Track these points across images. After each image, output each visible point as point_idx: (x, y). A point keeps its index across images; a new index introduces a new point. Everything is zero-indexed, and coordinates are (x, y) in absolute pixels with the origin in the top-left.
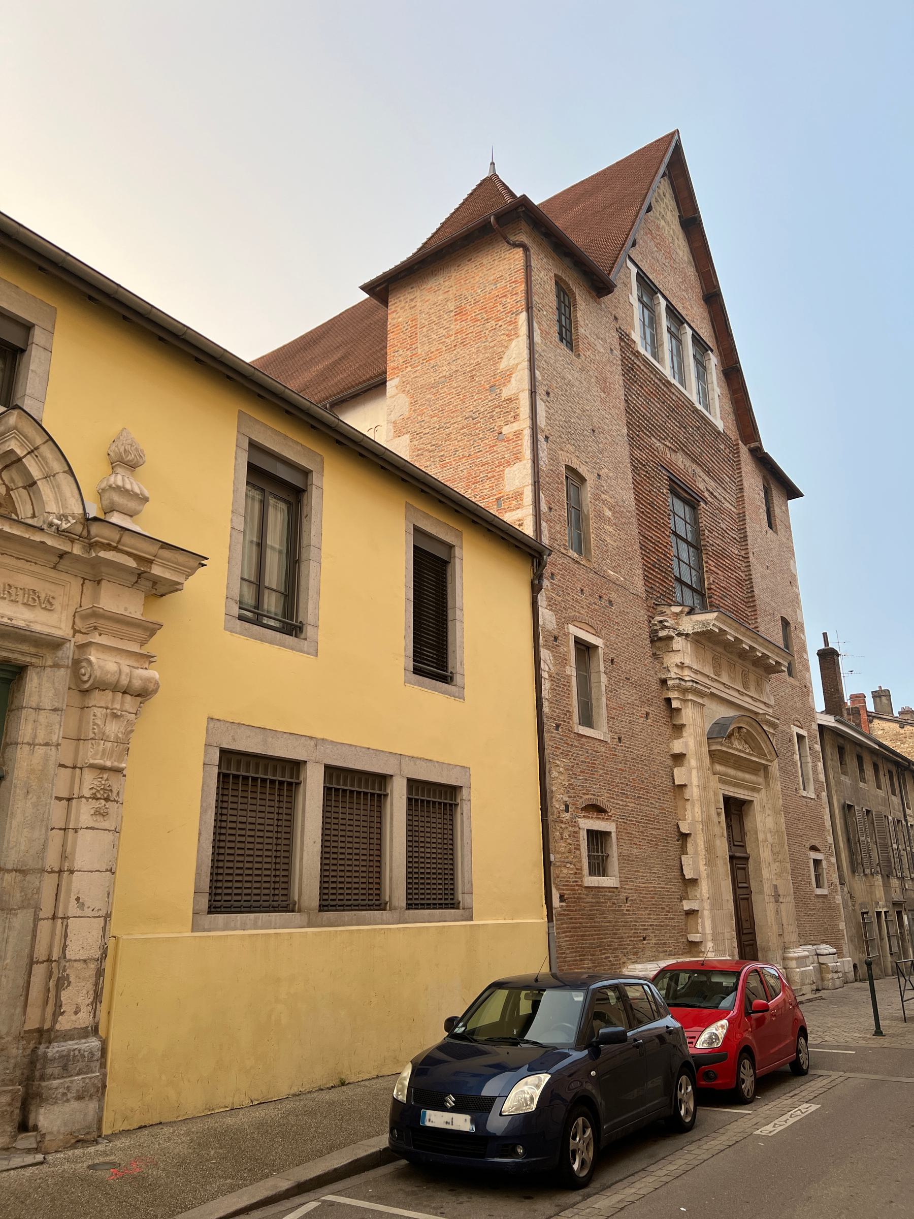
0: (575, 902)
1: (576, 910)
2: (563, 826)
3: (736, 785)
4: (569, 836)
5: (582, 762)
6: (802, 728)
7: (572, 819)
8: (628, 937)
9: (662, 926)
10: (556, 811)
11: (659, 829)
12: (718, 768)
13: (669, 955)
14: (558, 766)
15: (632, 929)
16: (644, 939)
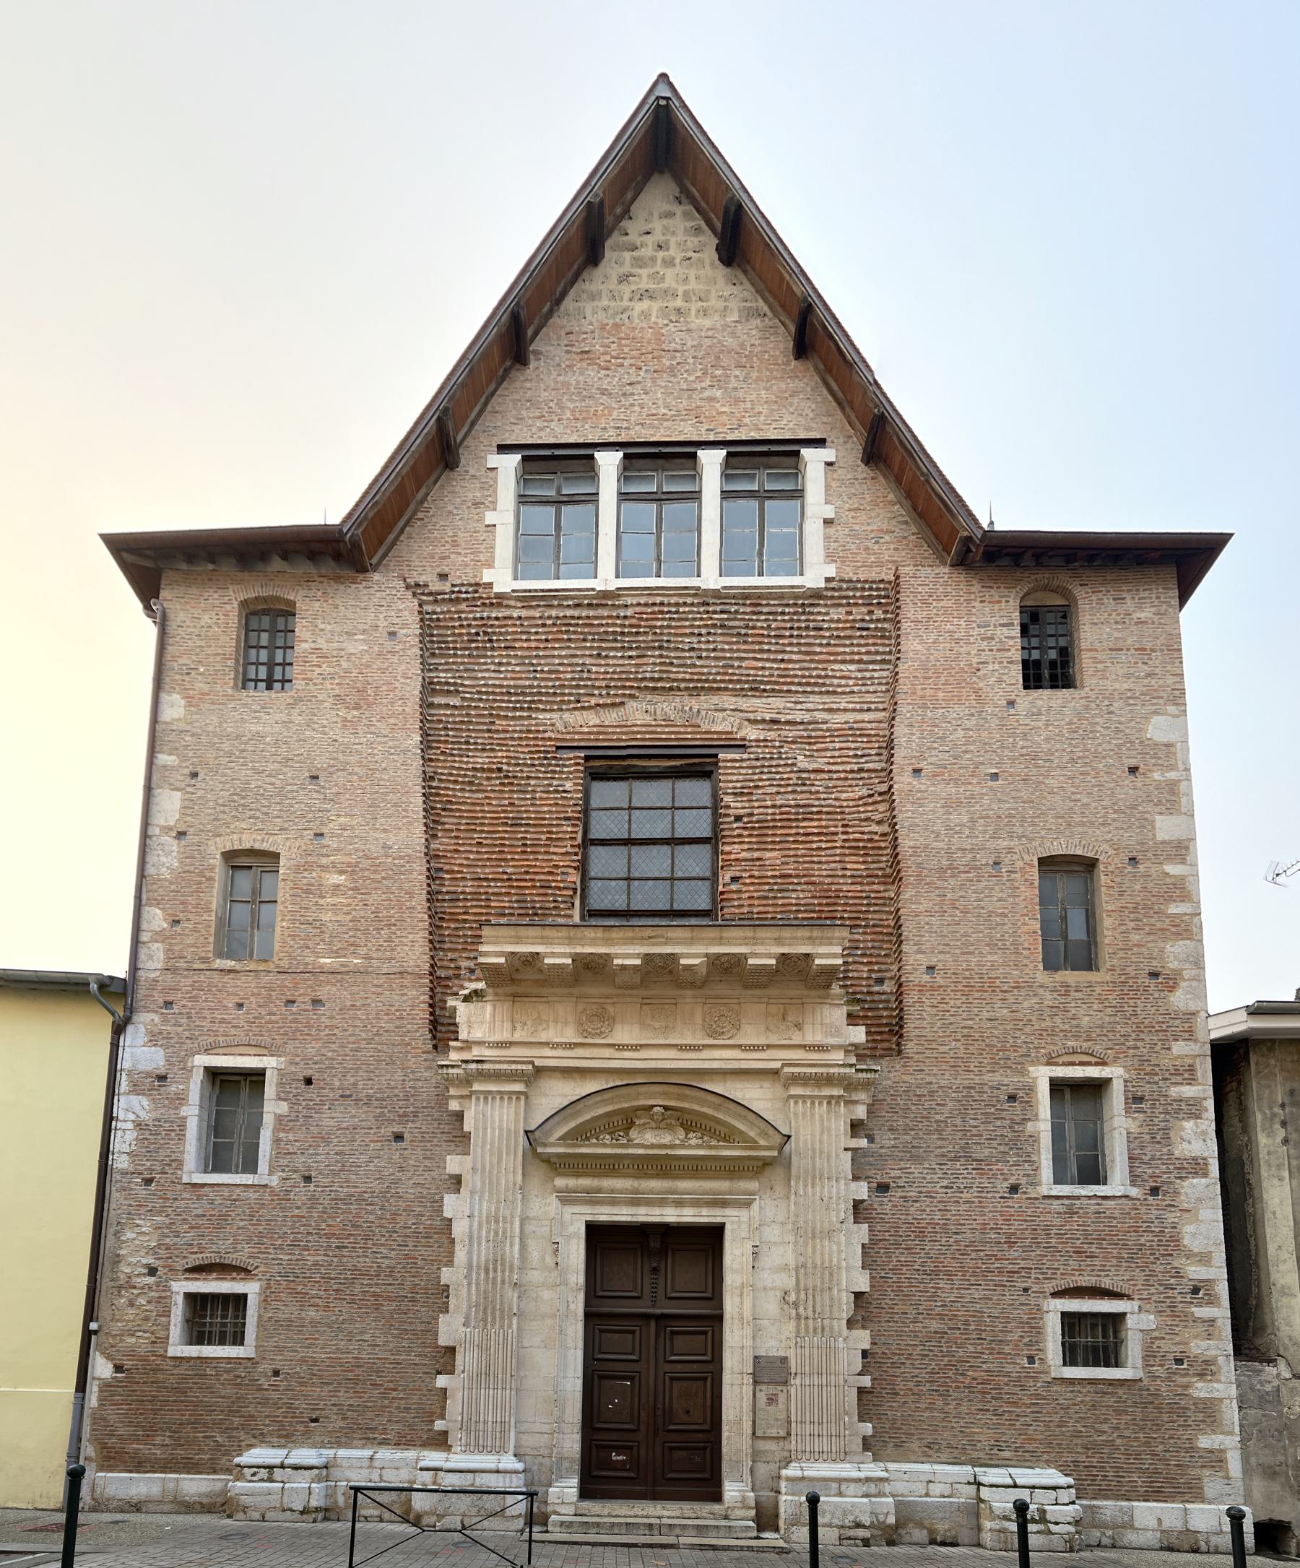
0: (145, 1373)
1: (144, 1382)
2: (135, 1292)
3: (635, 1203)
4: (149, 1302)
5: (196, 1216)
6: (1104, 1063)
7: (158, 1284)
8: (267, 1416)
9: (366, 1407)
10: (122, 1276)
11: (390, 1284)
12: (560, 1182)
13: (380, 1444)
14: (138, 1226)
15: (279, 1408)
16: (316, 1420)
